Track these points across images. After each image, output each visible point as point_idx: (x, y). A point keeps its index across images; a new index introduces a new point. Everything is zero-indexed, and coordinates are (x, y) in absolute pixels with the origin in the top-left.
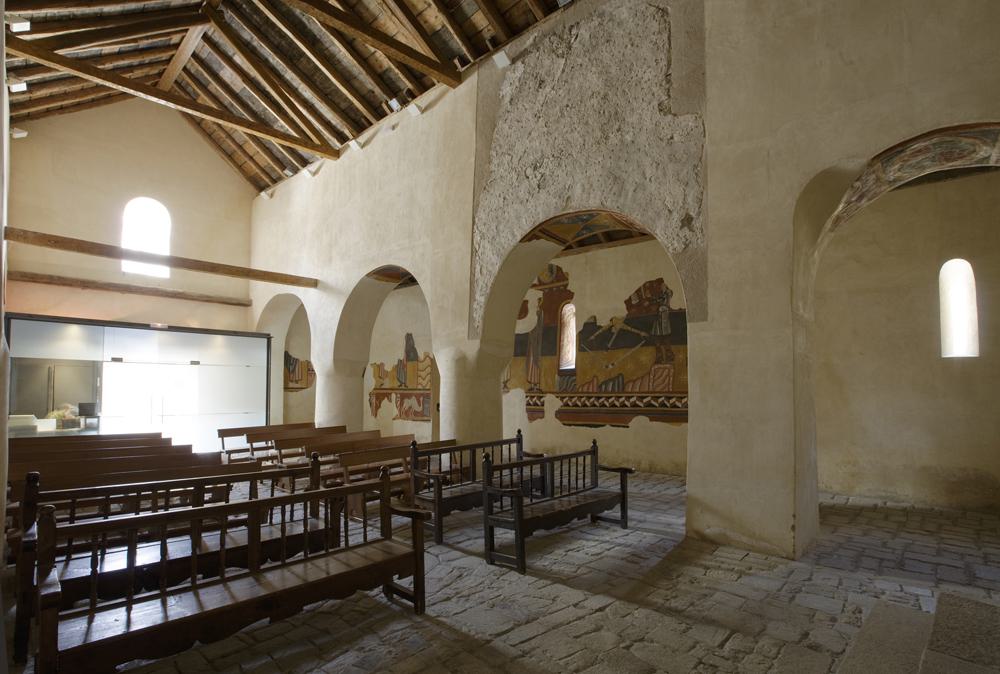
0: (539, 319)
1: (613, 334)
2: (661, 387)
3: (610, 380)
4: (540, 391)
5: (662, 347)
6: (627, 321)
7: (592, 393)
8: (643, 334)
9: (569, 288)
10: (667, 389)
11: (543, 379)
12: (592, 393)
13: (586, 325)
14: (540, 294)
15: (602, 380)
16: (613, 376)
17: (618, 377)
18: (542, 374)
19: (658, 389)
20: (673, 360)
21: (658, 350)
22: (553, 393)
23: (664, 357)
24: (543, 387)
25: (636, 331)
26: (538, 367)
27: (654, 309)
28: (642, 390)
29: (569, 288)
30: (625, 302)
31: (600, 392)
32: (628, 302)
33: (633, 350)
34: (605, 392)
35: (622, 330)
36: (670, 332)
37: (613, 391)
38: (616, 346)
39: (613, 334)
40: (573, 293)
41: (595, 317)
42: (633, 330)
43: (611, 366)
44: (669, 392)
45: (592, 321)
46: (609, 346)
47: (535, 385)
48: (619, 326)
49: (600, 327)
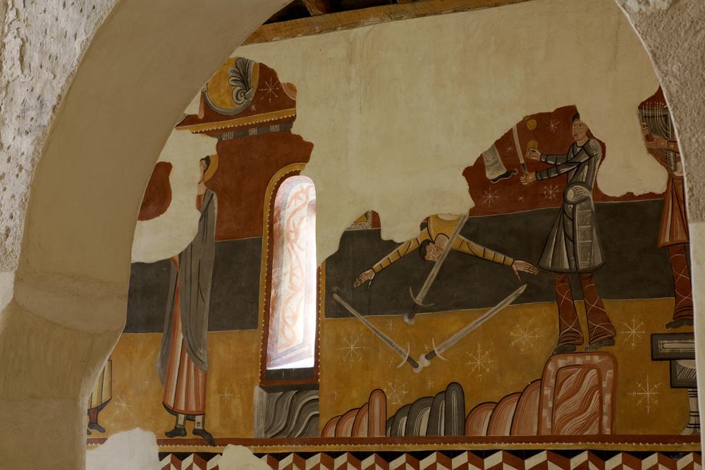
0: (204, 219)
1: (433, 263)
2: (580, 420)
3: (421, 402)
4: (205, 436)
5: (579, 306)
6: (472, 228)
7: (370, 440)
8: (520, 266)
9: (295, 130)
10: (593, 430)
11: (214, 402)
12: (370, 440)
13: (347, 237)
14: (209, 146)
15: (396, 401)
16: (434, 385)
17: (445, 393)
18: (213, 384)
19: (567, 430)
20: (611, 341)
21: (566, 313)
22: (246, 442)
23: (585, 334)
24: (214, 425)
25: (500, 257)
26: (199, 362)
27: (551, 192)
28: (523, 433)
29: (295, 130)
30: (468, 173)
31: (393, 439)
32: (474, 174)
33: (492, 312)
34: (406, 440)
35: (455, 254)
36: (598, 259)
37: (431, 436)
38: (441, 301)
39: (433, 263)
40: (309, 147)
41: (375, 216)
42: (490, 254)
43: (424, 362)
44: (601, 438)
45: (367, 225)
46: (419, 300)
47: (190, 417)
48: (451, 241)
49: (391, 245)
